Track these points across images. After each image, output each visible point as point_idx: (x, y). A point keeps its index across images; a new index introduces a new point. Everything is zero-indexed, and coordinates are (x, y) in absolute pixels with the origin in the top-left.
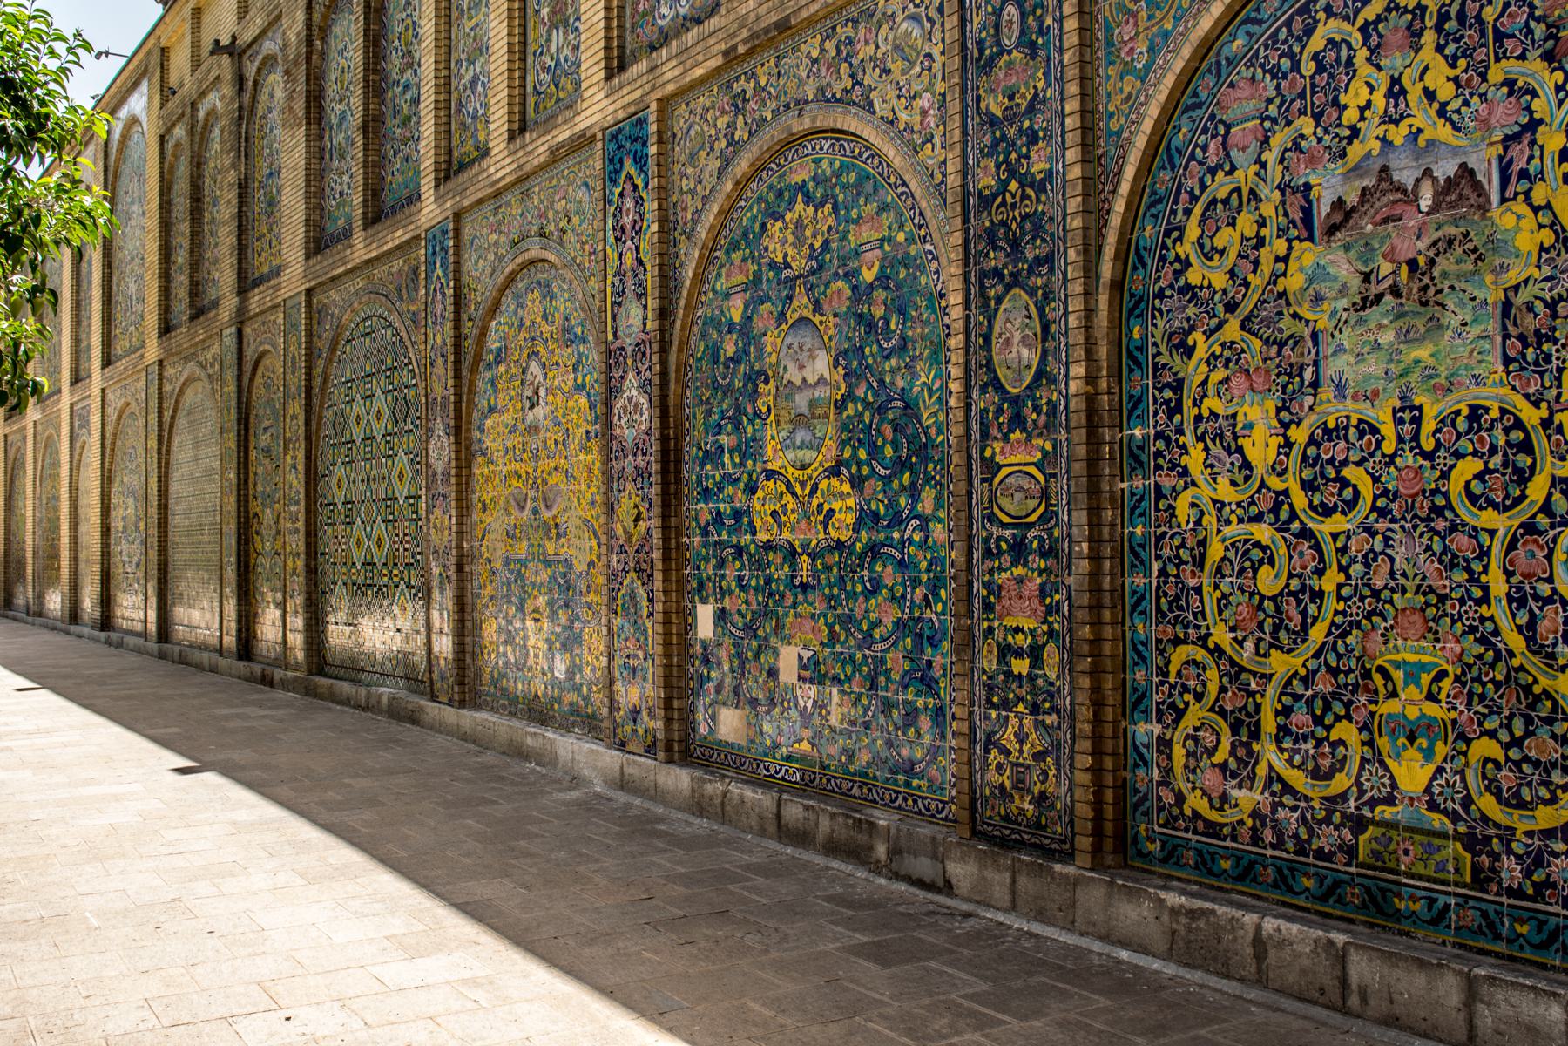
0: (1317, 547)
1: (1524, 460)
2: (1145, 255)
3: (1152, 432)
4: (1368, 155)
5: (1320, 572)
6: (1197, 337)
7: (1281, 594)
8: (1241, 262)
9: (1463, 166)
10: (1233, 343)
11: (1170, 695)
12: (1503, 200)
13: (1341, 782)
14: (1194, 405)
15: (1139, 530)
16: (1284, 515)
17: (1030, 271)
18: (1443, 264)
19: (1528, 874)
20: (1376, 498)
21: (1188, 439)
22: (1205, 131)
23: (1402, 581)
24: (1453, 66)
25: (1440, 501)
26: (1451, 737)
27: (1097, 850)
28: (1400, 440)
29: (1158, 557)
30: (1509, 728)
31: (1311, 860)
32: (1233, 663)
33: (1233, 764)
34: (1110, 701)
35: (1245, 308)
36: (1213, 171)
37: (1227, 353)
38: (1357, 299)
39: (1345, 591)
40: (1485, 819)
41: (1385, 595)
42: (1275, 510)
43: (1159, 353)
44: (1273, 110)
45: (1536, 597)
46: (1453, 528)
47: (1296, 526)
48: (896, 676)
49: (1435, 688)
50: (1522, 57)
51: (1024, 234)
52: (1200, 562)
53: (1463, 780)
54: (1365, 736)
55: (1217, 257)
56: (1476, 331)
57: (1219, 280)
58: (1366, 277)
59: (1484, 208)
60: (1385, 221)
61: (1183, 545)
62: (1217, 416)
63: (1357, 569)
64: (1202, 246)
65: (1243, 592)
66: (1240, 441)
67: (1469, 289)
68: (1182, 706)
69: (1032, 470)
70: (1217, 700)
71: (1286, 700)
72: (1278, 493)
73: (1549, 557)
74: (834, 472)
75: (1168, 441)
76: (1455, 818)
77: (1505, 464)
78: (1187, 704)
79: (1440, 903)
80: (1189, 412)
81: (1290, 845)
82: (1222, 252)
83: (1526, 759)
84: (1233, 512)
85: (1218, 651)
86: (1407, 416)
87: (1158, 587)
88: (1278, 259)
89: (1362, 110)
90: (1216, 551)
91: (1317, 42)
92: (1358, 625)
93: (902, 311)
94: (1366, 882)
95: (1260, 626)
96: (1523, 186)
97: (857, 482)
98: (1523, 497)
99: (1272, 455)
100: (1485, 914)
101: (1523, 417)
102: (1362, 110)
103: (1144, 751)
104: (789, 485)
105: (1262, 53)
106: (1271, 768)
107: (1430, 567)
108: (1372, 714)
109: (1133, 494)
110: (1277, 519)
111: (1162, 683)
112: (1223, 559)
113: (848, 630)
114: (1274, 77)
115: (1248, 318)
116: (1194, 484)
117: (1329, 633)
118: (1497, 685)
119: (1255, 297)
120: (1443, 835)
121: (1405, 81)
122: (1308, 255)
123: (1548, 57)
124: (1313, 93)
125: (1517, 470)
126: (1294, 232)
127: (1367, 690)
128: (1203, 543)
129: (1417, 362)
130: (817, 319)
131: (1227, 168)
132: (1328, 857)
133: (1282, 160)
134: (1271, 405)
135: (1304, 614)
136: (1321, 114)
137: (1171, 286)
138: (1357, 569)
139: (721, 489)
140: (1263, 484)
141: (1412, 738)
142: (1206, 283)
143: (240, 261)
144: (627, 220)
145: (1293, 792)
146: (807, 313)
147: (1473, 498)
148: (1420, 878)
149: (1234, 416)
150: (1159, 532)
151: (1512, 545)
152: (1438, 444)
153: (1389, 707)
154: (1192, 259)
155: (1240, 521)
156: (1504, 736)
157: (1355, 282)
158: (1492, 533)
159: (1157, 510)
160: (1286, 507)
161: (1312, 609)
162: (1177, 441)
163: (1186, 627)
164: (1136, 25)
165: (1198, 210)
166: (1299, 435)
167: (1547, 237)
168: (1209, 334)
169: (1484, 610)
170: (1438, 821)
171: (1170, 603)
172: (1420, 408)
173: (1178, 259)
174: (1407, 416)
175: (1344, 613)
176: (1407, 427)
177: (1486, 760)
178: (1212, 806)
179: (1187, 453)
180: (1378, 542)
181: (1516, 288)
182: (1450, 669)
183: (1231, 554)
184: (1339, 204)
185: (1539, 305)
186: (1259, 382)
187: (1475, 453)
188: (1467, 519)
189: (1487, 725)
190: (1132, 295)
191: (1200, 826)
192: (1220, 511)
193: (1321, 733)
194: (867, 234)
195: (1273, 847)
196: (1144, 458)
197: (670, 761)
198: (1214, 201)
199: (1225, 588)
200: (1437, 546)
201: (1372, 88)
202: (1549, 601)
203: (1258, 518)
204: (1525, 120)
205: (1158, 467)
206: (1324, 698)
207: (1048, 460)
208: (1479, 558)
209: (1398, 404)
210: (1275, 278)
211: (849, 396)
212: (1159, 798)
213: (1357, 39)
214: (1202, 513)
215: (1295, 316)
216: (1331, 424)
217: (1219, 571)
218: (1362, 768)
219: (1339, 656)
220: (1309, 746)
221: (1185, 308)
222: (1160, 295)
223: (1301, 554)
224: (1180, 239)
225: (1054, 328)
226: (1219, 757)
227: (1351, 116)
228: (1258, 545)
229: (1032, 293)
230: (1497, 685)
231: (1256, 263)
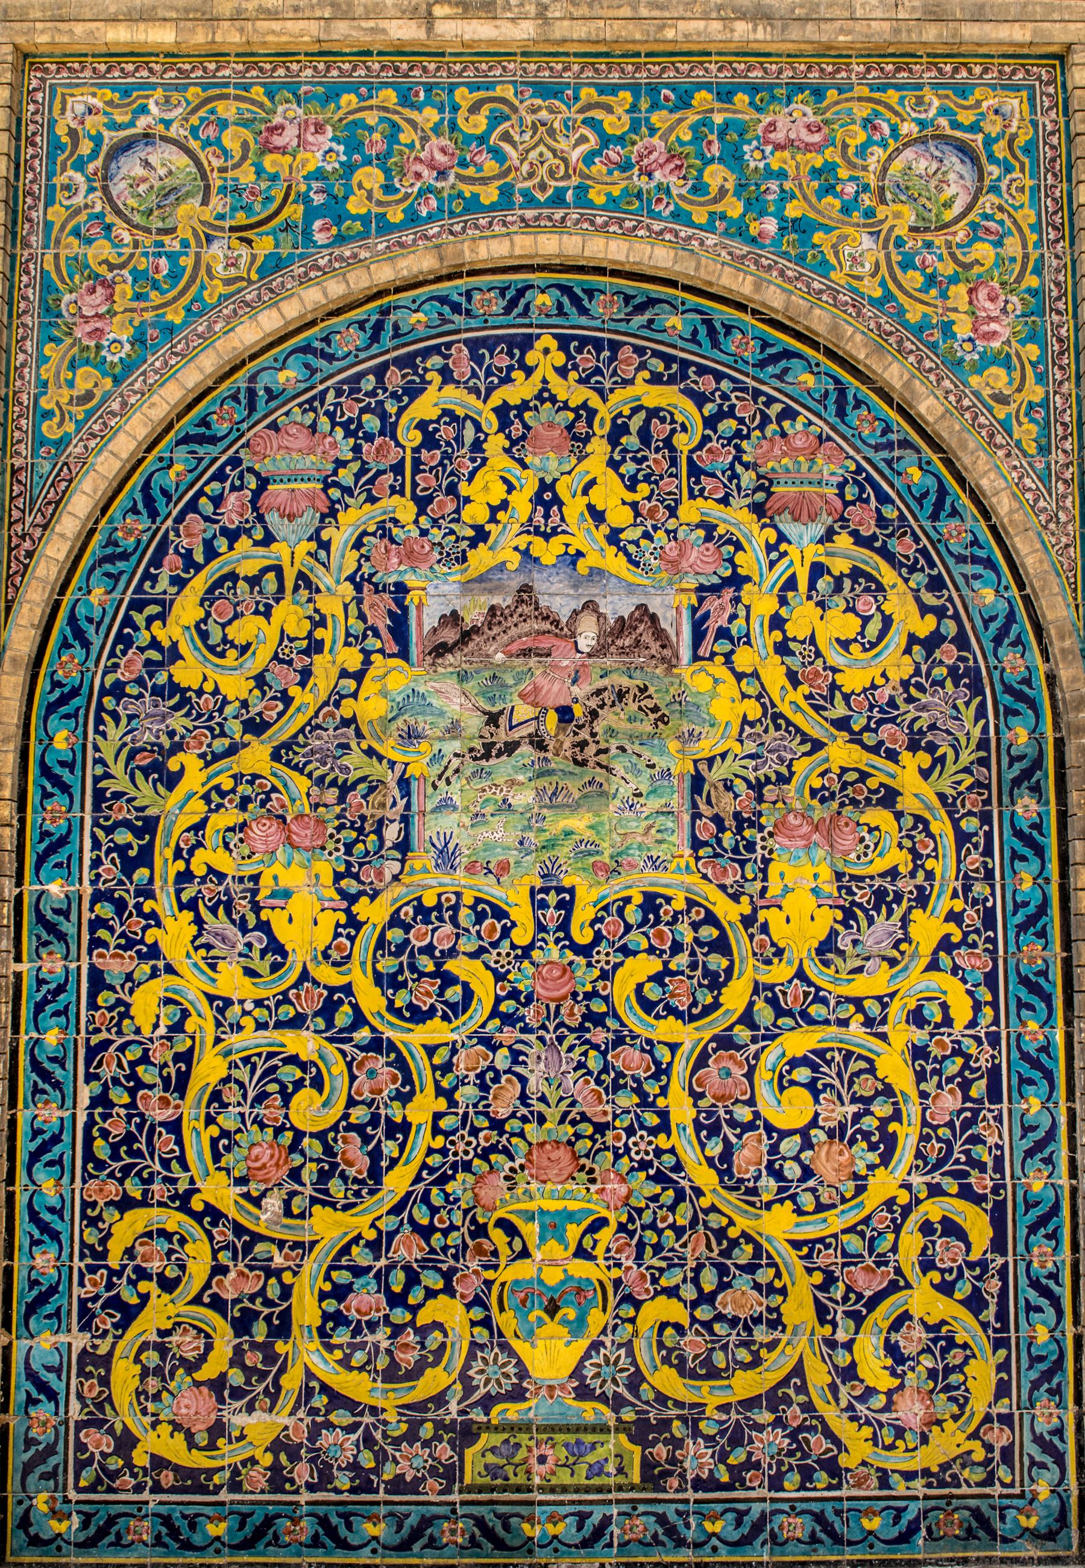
0: (401, 1063)
1: (717, 962)
2: (90, 630)
3: (88, 890)
4: (502, 567)
5: (405, 1098)
6: (189, 761)
7: (335, 1128)
8: (277, 668)
9: (642, 608)
10: (255, 776)
11: (110, 1286)
12: (696, 658)
13: (433, 1381)
14: (178, 854)
15: (52, 1038)
18: (608, 718)
19: (723, 1457)
20: (498, 1000)
21: (164, 903)
22: (220, 476)
23: (539, 1107)
24: (632, 488)
25: (599, 1007)
26: (612, 1302)
28: (541, 928)
29: (89, 1078)
30: (696, 1281)
31: (381, 1496)
32: (239, 1229)
33: (236, 1378)
36: (232, 536)
37: (244, 789)
38: (477, 744)
39: (444, 1124)
40: (662, 1399)
41: (513, 1125)
43: (107, 776)
45: (733, 1123)
46: (619, 1041)
47: (363, 1034)
49: (587, 1242)
50: (725, 501)
52: (181, 1084)
53: (631, 1353)
54: (477, 1313)
55: (232, 654)
56: (654, 804)
58: (493, 719)
59: (670, 663)
60: (526, 653)
61: (145, 1059)
62: (221, 876)
63: (467, 1093)
64: (204, 636)
65: (262, 1126)
66: (264, 915)
67: (646, 753)
68: (134, 1300)
70: (208, 1285)
71: (342, 1277)
72: (332, 990)
73: (750, 1075)
75: (120, 906)
76: (617, 1403)
77: (693, 966)
78: (145, 1298)
79: (596, 1518)
81: (343, 1481)
82: (244, 649)
83: (720, 1317)
84: (245, 1013)
85: (213, 1214)
86: (552, 899)
87: (90, 1123)
88: (344, 674)
89: (494, 510)
91: (425, 407)
92: (467, 1167)
94: (475, 1510)
95: (295, 1174)
96: (723, 646)
98: (716, 1005)
99: (323, 936)
100: (662, 1519)
101: (718, 911)
102: (494, 510)
103: (50, 1378)
105: (330, 397)
106: (309, 1375)
107: (583, 1091)
108: (489, 1283)
109: (41, 982)
110: (330, 1024)
111: (92, 1270)
112: (226, 1080)
114: (348, 434)
115: (287, 746)
116: (170, 970)
117: (418, 1179)
118: (679, 1231)
119: (301, 720)
120: (604, 1429)
121: (561, 489)
123: (758, 510)
124: (416, 471)
125: (707, 973)
126: (372, 643)
127: (479, 1251)
128: (186, 1057)
129: (568, 833)
131: (259, 535)
132: (414, 1487)
133: (358, 545)
134: (325, 869)
135: (376, 1155)
136: (430, 499)
137: (140, 682)
138: (467, 1093)
140: (305, 975)
141: (552, 1309)
142: (209, 687)
145: (351, 1405)
147: (647, 1006)
148: (565, 1489)
149: (256, 878)
150: (95, 1040)
151: (702, 1061)
152: (598, 938)
153: (512, 1273)
154: (183, 649)
155: (261, 1026)
156: (689, 1293)
157: (474, 723)
158: (673, 1047)
159: (93, 1005)
160: (346, 1008)
161: (390, 1148)
162: (138, 906)
163: (150, 1181)
164: (110, 298)
165: (199, 583)
167: (754, 710)
169: (662, 1141)
170: (590, 1411)
171: (115, 1148)
172: (571, 891)
173: (155, 644)
174: (552, 899)
175: (443, 1152)
177: (663, 1326)
178: (191, 1444)
179: (159, 924)
180: (502, 1061)
181: (711, 761)
182: (612, 1217)
183: (243, 1074)
184: (452, 619)
185: (740, 786)
186: (303, 834)
187: (651, 950)
188: (638, 1030)
189: (664, 1282)
190: (56, 684)
191: (167, 1478)
192: (221, 1011)
195: (311, 1487)
198: (233, 577)
199: (228, 1121)
200: (594, 1062)
201: (511, 488)
202: (751, 1126)
203: (297, 1022)
204: (728, 573)
205: (96, 943)
206: (407, 1269)
208: (656, 1076)
209: (539, 883)
210: (337, 699)
212: (81, 1447)
213: (491, 422)
214: (185, 1014)
215: (370, 752)
216: (429, 901)
217: (216, 1096)
218: (471, 1356)
219: (434, 1210)
220: (382, 1336)
221: (164, 718)
222: (118, 690)
223: (372, 1073)
224: (162, 617)
226: (208, 1371)
227: (476, 513)
228: (293, 1060)
230: (679, 1231)
231: (306, 674)
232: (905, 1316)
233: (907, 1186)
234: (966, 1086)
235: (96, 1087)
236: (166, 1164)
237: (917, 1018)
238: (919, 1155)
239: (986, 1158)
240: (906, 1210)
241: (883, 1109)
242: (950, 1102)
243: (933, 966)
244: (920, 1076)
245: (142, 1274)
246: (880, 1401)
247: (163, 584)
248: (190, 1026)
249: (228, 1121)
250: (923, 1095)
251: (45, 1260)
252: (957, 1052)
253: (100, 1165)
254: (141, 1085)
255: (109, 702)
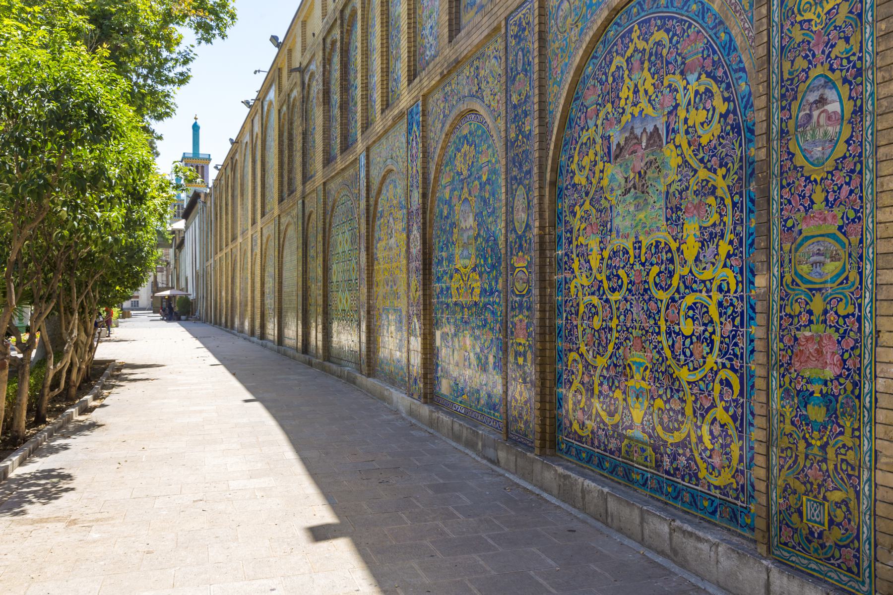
1: (671, 267)
5: (611, 319)
12: (667, 143)
15: (560, 298)
16: (601, 292)
18: (650, 174)
27: (542, 447)
34: (548, 378)
35: (591, 195)
36: (582, 130)
42: (599, 290)
44: (600, 101)
52: (577, 314)
57: (584, 181)
59: (661, 147)
63: (622, 317)
69: (524, 270)
73: (678, 313)
80: (575, 243)
81: (602, 448)
82: (584, 168)
85: (581, 355)
86: (637, 245)
90: (582, 309)
98: (671, 285)
122: (610, 169)
128: (578, 305)
134: (598, 239)
140: (595, 278)
143: (303, 169)
144: (414, 152)
153: (631, 383)
157: (623, 181)
166: (606, 254)
174: (637, 245)
176: (637, 251)
184: (618, 145)
193: (611, 395)
198: (582, 144)
202: (678, 334)
204: (674, 104)
211: (478, 234)
215: (606, 198)
222: (567, 188)
232: (715, 419)
233: (716, 363)
234: (733, 320)
237: (720, 290)
238: (720, 350)
239: (739, 353)
240: (716, 373)
241: (710, 329)
242: (729, 327)
243: (725, 266)
244: (721, 316)
246: (708, 453)
250: (721, 323)
252: (732, 305)
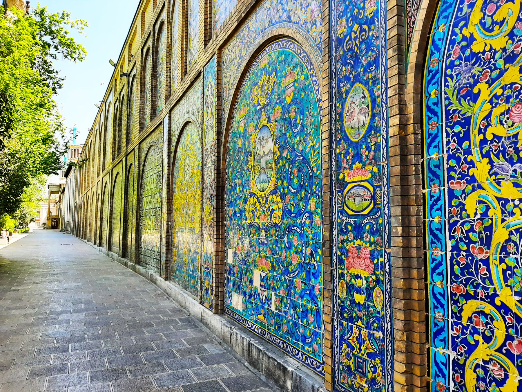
3: (446, 155)
6: (482, 86)
10: (512, 84)
11: (463, 333)
14: (480, 132)
15: (436, 220)
17: (365, 71)
21: (476, 156)
29: (451, 237)
34: (417, 330)
37: (508, 92)
43: (450, 104)
48: (298, 291)
51: (361, 52)
52: (487, 242)
55: (497, 27)
61: (472, 230)
62: (499, 138)
68: (473, 343)
70: (504, 344)
74: (274, 192)
75: (458, 160)
78: (477, 342)
80: (475, 138)
82: (502, 23)
84: (515, 206)
85: (504, 309)
87: (452, 258)
93: (302, 113)
97: (283, 196)
104: (258, 199)
109: (432, 196)
111: (457, 324)
112: (508, 241)
113: (279, 266)
116: (480, 187)
128: (489, 229)
130: (268, 126)
137: (460, 58)
139: (236, 201)
142: (488, 48)
143: (127, 138)
146: (265, 123)
150: (452, 221)
154: (475, 36)
159: (450, 206)
162: (465, 159)
163: (476, 287)
168: (490, 83)
171: (462, 269)
179: (474, 166)
190: (430, 71)
192: (504, 205)
194: (288, 80)
196: (439, 173)
197: (216, 313)
199: (510, 261)
205: (450, 178)
207: (376, 177)
211: (281, 157)
214: (488, 208)
217: (504, 249)
221: (470, 70)
222: (452, 66)
224: (466, 25)
225: (379, 100)
229: (366, 83)
235: (453, 242)
236: (483, 280)
245: (475, 331)
247: (465, 10)
248: (490, 213)
249: (510, 261)
251: (439, 314)
253: (457, 277)
254: (471, 242)
255: (449, 72)
